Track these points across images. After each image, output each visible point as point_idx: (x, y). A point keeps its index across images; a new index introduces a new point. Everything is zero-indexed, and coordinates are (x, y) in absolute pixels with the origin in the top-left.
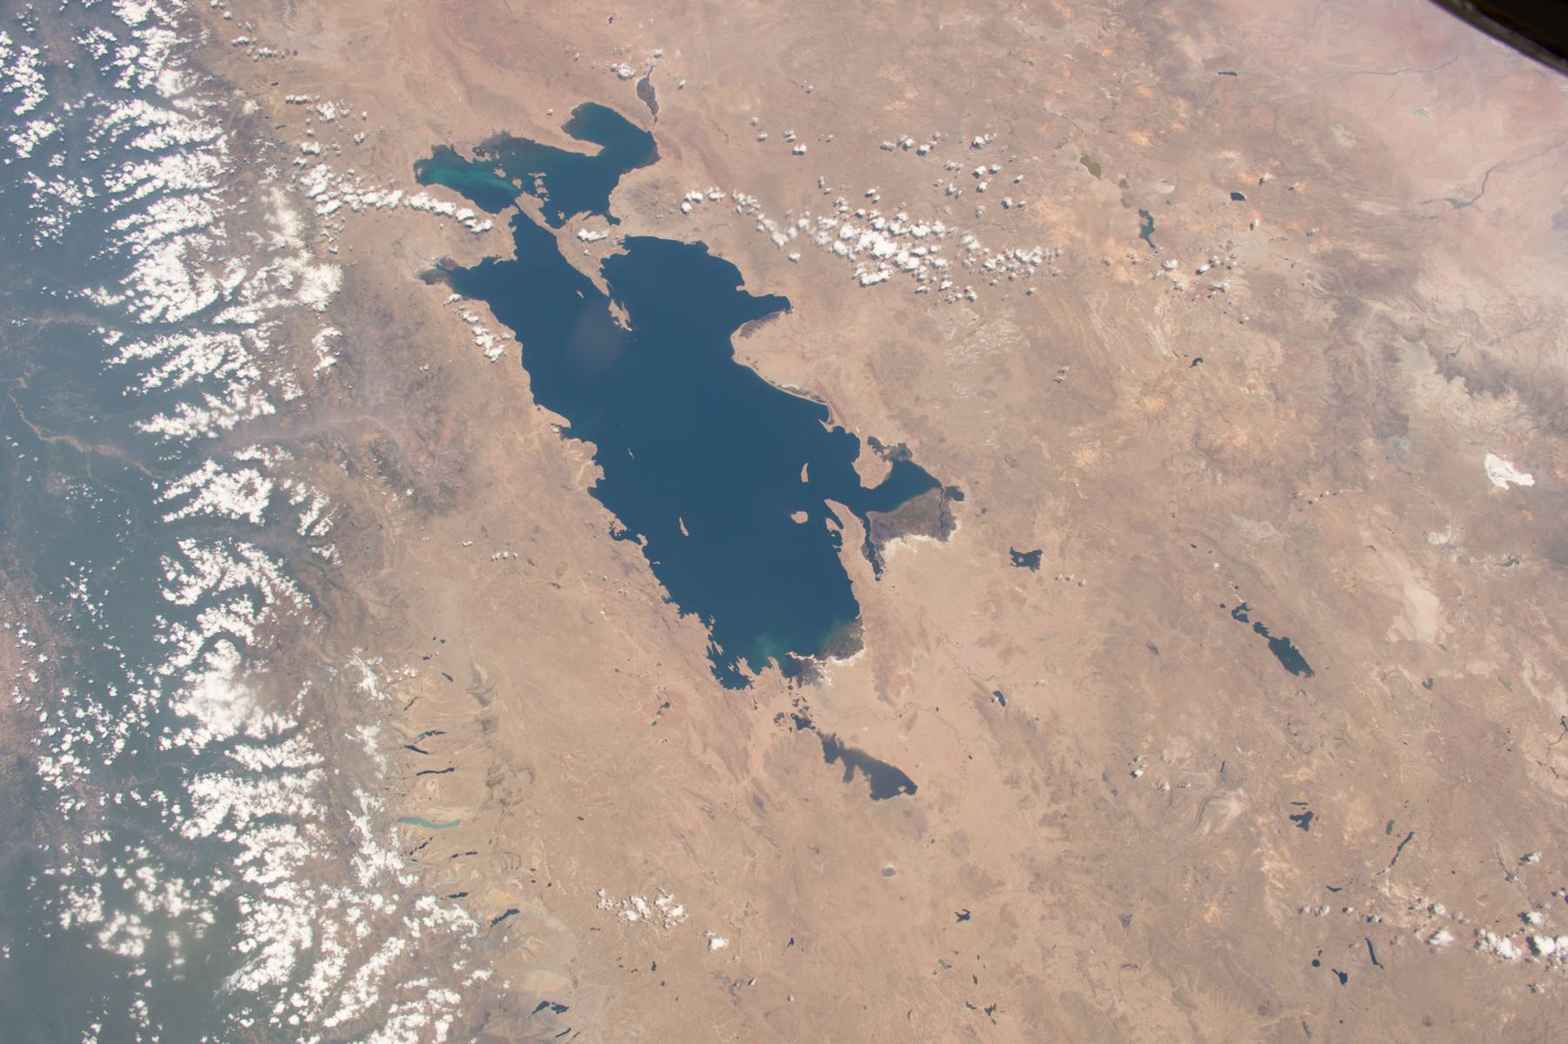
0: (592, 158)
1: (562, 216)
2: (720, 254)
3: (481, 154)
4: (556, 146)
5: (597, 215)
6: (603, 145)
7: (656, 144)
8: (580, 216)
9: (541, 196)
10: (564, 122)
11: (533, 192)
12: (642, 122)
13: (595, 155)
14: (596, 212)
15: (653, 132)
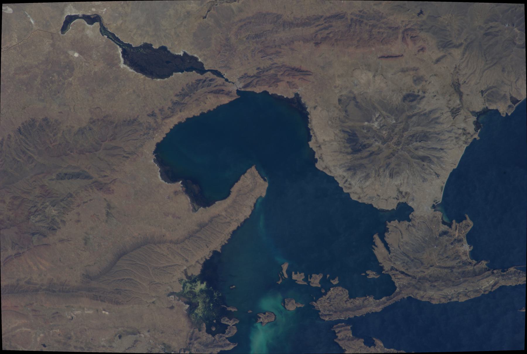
0: (268, 190)
1: (372, 275)
2: (514, 101)
3: (223, 328)
4: (234, 226)
5: (386, 230)
6: (250, 167)
7: (265, 93)
8: (380, 251)
9: (326, 285)
10: (185, 200)
11: (318, 293)
12: (219, 92)
13: (266, 185)
14: (383, 232)
15: (240, 86)
